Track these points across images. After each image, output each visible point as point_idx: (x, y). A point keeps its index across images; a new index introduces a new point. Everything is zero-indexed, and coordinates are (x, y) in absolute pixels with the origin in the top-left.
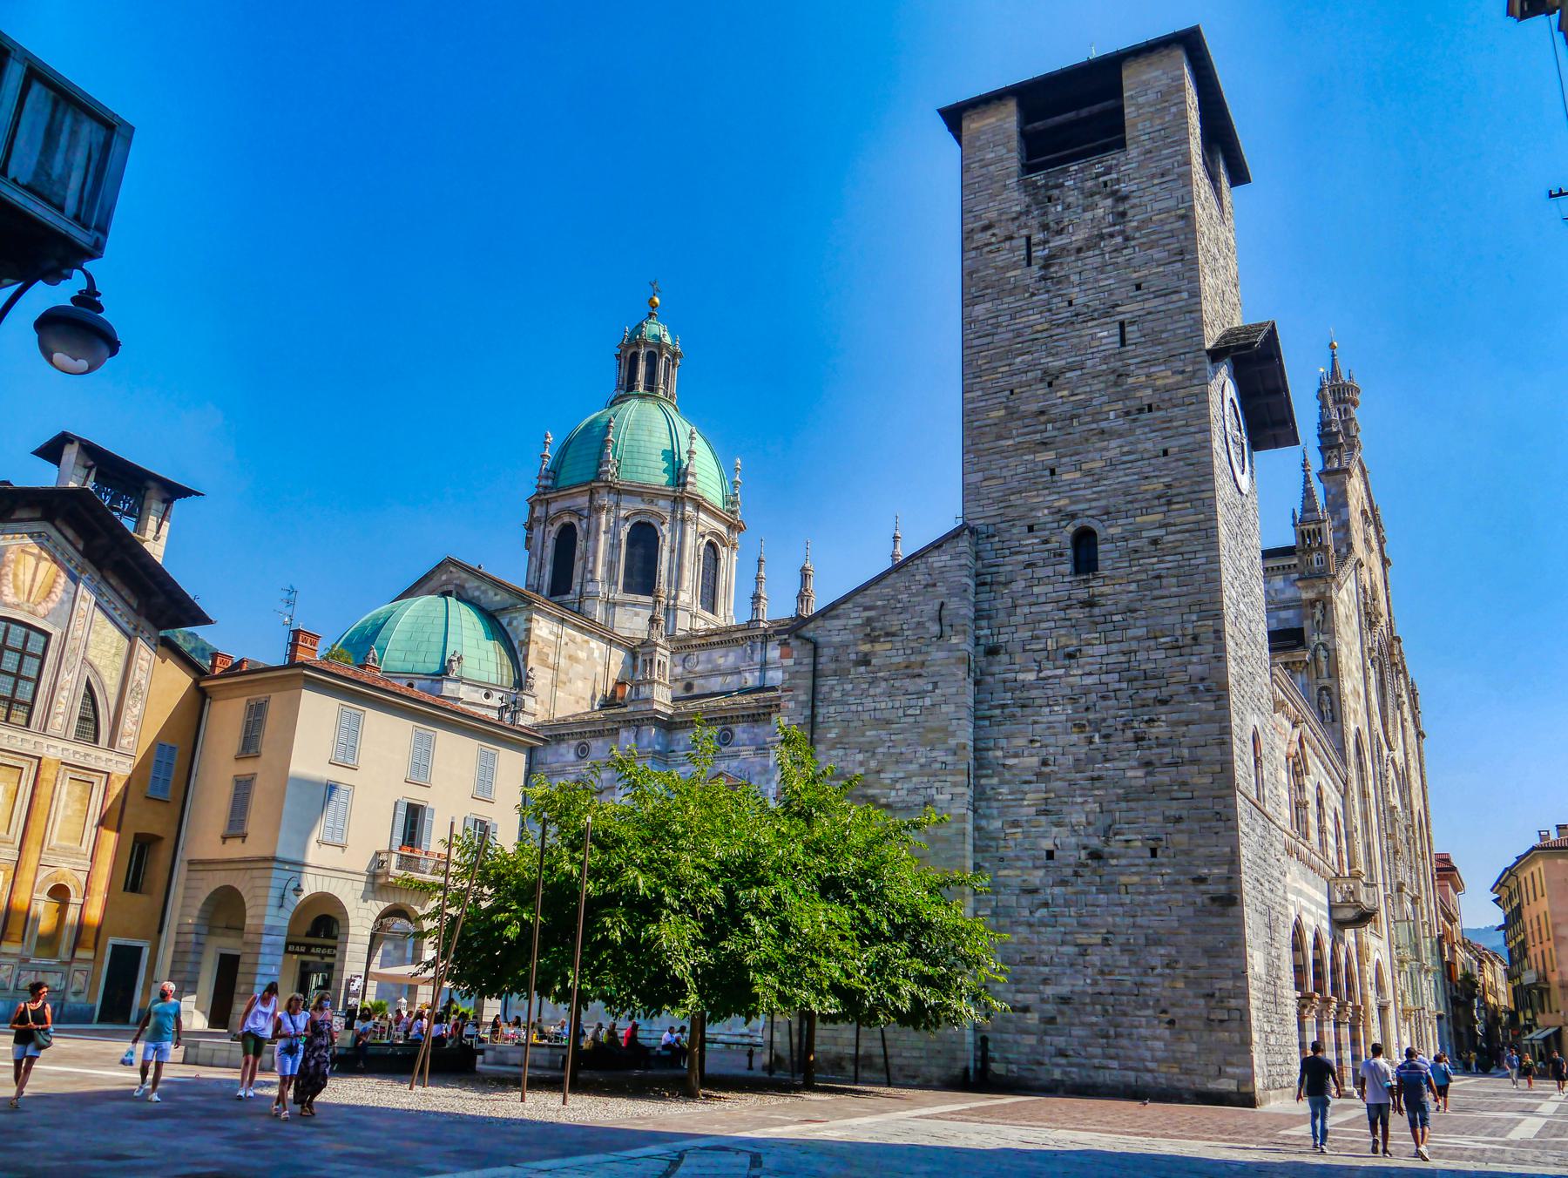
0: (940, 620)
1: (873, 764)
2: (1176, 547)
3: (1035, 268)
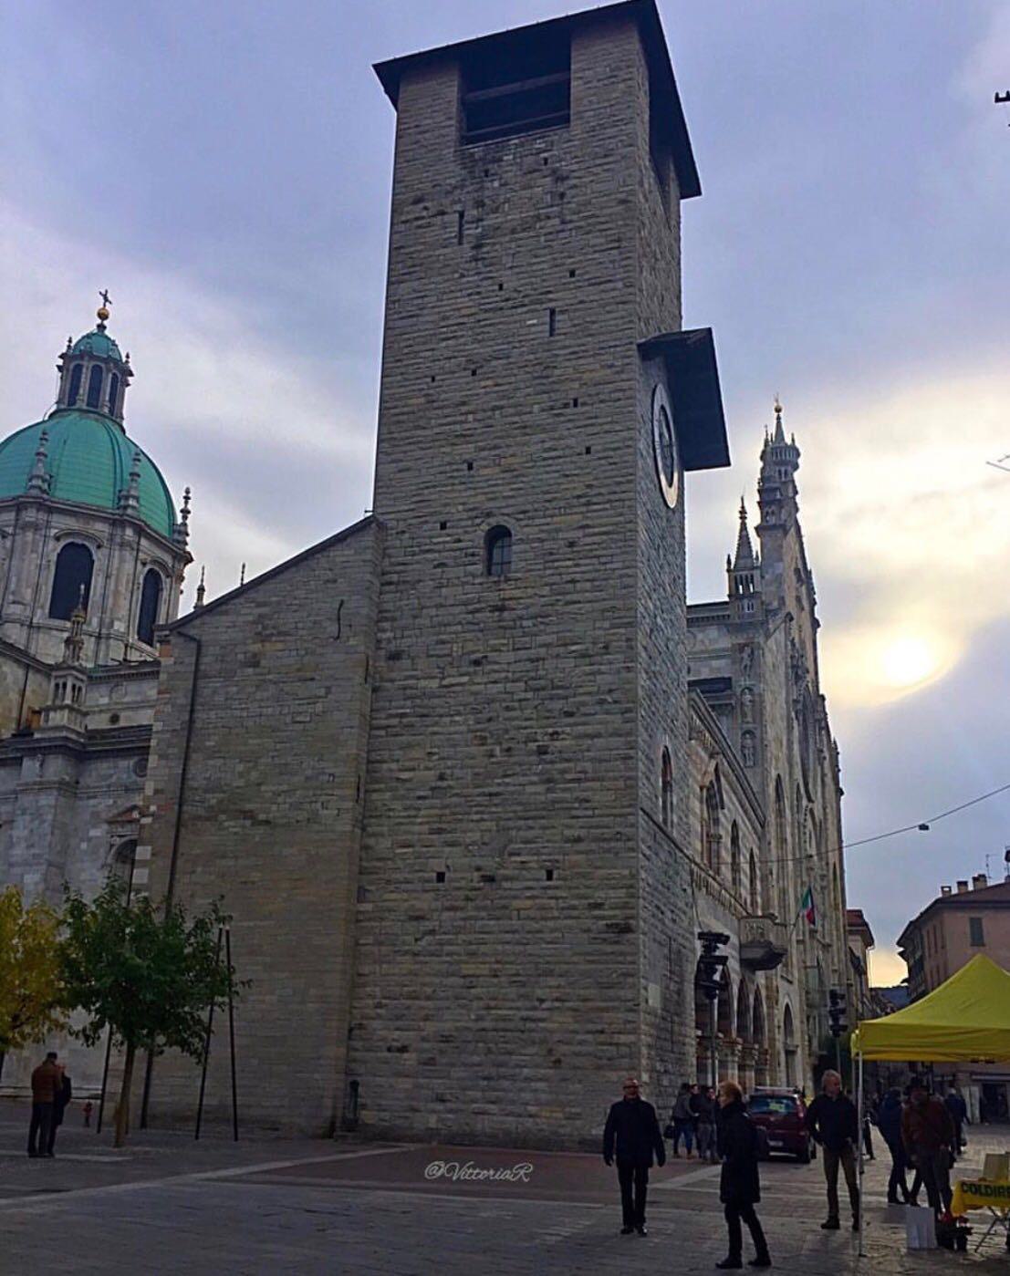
0: (339, 619)
1: (254, 775)
3: (466, 246)
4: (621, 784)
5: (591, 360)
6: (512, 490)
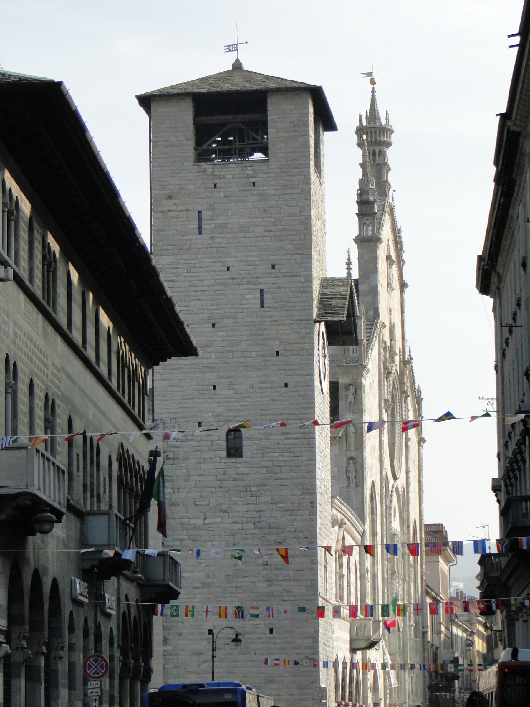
2: (290, 448)
4: (309, 583)
5: (286, 327)
6: (242, 406)
